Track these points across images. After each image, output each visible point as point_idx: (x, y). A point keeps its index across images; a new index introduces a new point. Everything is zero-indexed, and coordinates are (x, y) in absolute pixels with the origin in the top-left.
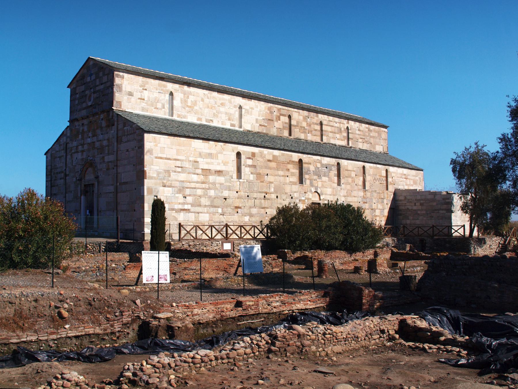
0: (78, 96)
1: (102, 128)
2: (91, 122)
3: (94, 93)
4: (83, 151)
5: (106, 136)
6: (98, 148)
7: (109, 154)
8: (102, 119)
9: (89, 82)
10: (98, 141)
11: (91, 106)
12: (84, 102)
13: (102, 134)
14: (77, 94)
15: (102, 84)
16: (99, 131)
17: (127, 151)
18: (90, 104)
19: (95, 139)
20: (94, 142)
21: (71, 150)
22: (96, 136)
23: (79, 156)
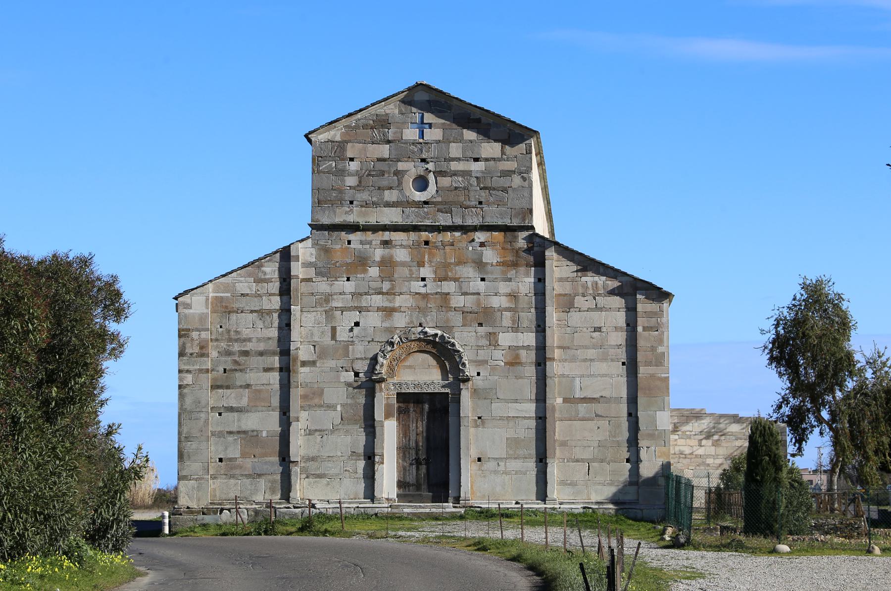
0: (354, 166)
1: (480, 265)
2: (427, 243)
3: (439, 173)
4: (389, 312)
5: (504, 288)
6: (466, 310)
7: (516, 329)
8: (482, 245)
9: (414, 143)
10: (465, 294)
11: (426, 203)
12: (391, 188)
13: (483, 279)
14: (352, 159)
15: (476, 160)
16: (468, 272)
17: (598, 329)
18: (419, 196)
19: (449, 287)
20: (448, 294)
21: (327, 301)
22: (456, 280)
23: (372, 320)
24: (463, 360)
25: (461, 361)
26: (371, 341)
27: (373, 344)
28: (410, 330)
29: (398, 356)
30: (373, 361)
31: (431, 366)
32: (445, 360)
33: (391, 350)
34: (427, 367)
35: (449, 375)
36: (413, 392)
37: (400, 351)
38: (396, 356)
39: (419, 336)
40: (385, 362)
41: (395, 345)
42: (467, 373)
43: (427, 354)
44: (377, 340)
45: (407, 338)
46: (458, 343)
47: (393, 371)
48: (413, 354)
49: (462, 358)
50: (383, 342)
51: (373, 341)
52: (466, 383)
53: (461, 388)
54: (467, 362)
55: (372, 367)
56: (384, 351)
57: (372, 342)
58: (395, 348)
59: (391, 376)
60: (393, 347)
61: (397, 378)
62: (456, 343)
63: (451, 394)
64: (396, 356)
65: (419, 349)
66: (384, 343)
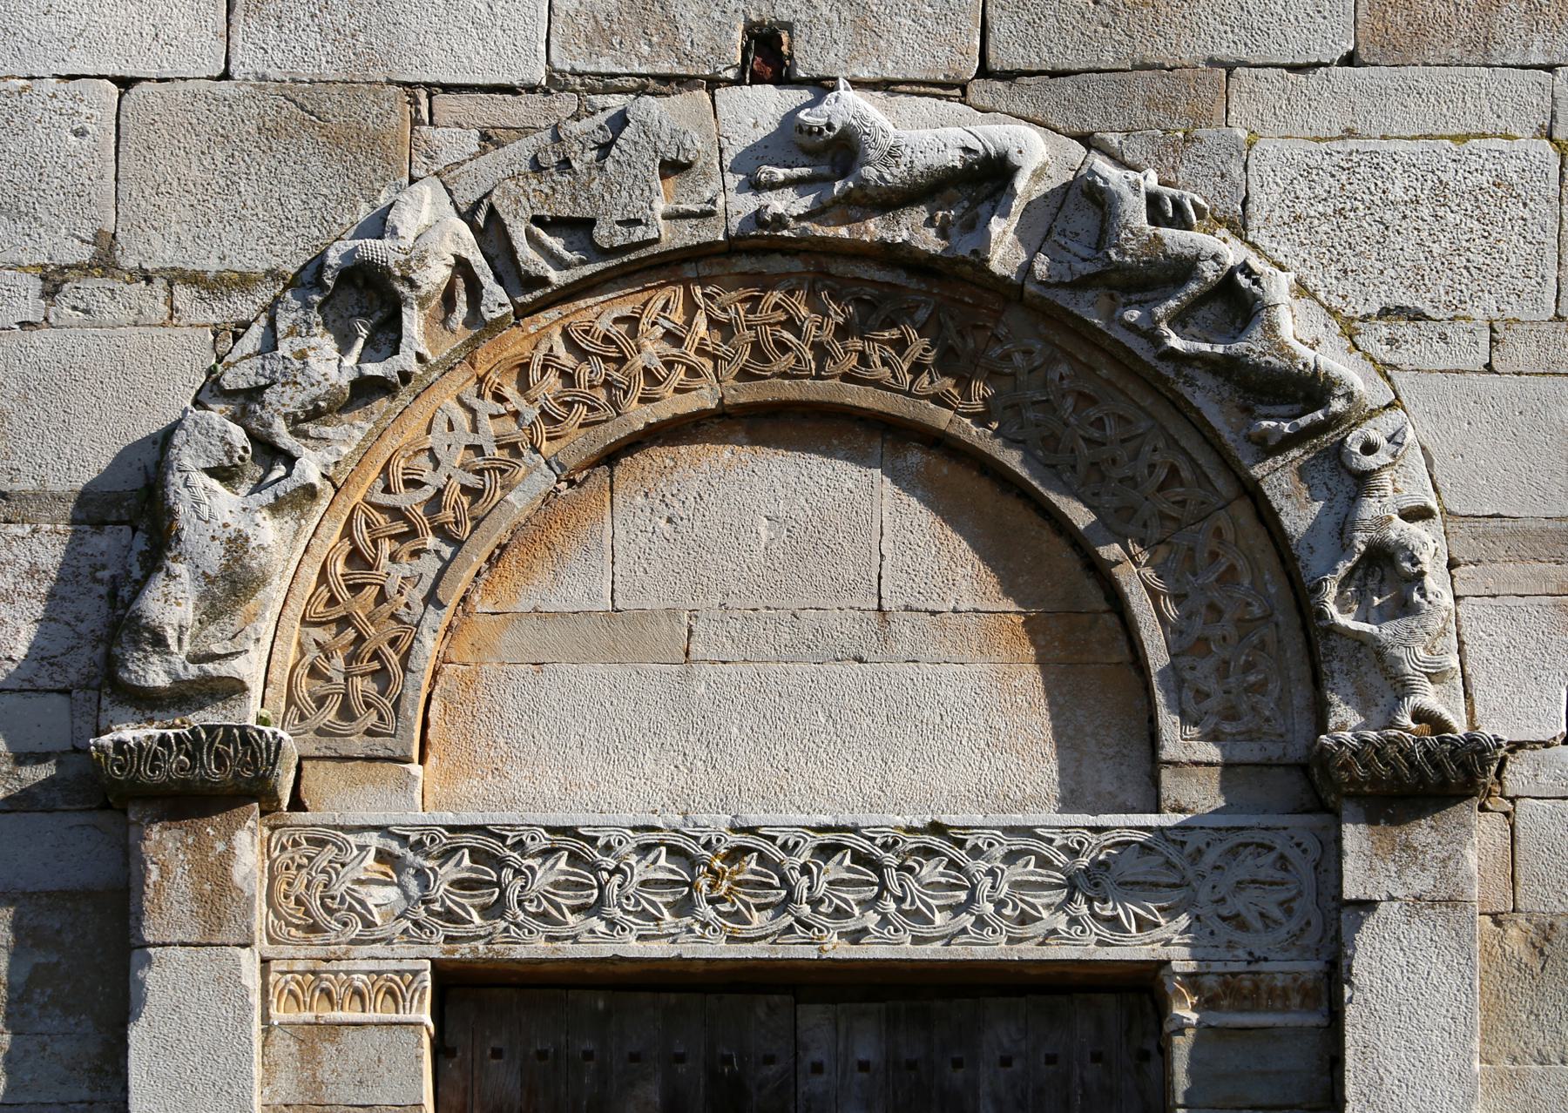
24: (1370, 508)
25: (1343, 529)
26: (85, 269)
27: (110, 310)
28: (620, 121)
29: (453, 474)
30: (103, 543)
31: (903, 627)
32: (1115, 524)
33: (365, 390)
34: (847, 627)
35: (1168, 722)
36: (658, 950)
37: (488, 406)
38: (434, 480)
39: (748, 203)
40: (269, 532)
41: (413, 322)
42: (1429, 697)
43: (860, 457)
44: (163, 255)
45: (577, 228)
46: (1302, 289)
47: (382, 676)
48: (660, 456)
49: (1363, 482)
50: (244, 282)
51: (105, 262)
52: (1422, 832)
53: (1351, 891)
54: (1427, 542)
55: (93, 612)
56: (254, 393)
57: (94, 291)
58: (405, 360)
59: (358, 744)
60: (388, 335)
61: (449, 777)
62: (1278, 288)
63: (1192, 981)
64: (434, 480)
65: (747, 394)
66: (264, 295)
